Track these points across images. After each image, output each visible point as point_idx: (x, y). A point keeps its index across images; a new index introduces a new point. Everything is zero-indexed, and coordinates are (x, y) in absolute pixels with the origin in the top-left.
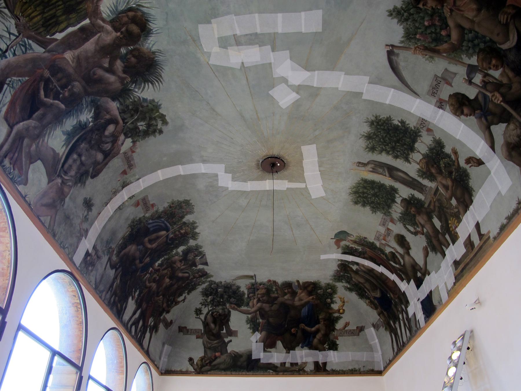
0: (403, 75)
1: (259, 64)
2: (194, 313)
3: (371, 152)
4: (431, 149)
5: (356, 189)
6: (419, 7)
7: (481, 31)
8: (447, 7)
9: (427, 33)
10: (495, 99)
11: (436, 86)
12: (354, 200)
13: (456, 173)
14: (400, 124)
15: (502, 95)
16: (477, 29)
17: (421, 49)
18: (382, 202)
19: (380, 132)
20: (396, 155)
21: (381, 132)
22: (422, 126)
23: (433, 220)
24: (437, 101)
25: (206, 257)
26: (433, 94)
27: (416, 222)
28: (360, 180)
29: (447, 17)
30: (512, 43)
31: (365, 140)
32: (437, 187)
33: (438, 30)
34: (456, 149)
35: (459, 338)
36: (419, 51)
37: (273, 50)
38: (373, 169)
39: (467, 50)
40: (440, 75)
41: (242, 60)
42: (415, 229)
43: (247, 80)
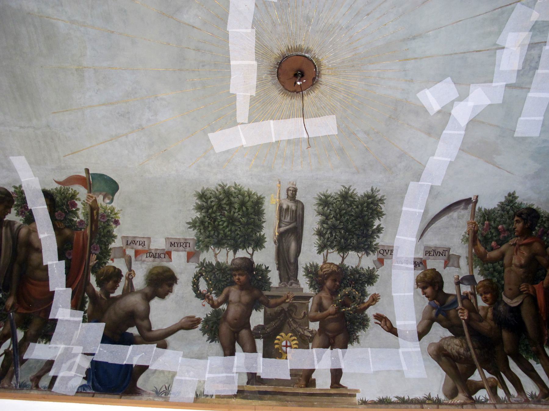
0: (442, 217)
1: (496, 69)
4: (356, 271)
5: (235, 193)
6: (515, 217)
7: (506, 275)
8: (517, 240)
9: (491, 230)
10: (460, 312)
11: (438, 252)
12: (208, 193)
13: (350, 310)
14: (375, 227)
15: (469, 316)
16: (506, 270)
17: (474, 228)
18: (222, 232)
19: (357, 207)
20: (324, 232)
21: (356, 209)
22: (382, 252)
23: (254, 311)
24: (421, 259)
26: (427, 252)
27: (224, 287)
28: (259, 195)
29: (508, 243)
30: (512, 304)
31: (341, 192)
32: (310, 297)
33: (495, 238)
34: (379, 299)
36: (472, 227)
37: (508, 86)
38: (288, 209)
39: (485, 269)
40: (451, 253)
41: (507, 48)
43: (477, 51)
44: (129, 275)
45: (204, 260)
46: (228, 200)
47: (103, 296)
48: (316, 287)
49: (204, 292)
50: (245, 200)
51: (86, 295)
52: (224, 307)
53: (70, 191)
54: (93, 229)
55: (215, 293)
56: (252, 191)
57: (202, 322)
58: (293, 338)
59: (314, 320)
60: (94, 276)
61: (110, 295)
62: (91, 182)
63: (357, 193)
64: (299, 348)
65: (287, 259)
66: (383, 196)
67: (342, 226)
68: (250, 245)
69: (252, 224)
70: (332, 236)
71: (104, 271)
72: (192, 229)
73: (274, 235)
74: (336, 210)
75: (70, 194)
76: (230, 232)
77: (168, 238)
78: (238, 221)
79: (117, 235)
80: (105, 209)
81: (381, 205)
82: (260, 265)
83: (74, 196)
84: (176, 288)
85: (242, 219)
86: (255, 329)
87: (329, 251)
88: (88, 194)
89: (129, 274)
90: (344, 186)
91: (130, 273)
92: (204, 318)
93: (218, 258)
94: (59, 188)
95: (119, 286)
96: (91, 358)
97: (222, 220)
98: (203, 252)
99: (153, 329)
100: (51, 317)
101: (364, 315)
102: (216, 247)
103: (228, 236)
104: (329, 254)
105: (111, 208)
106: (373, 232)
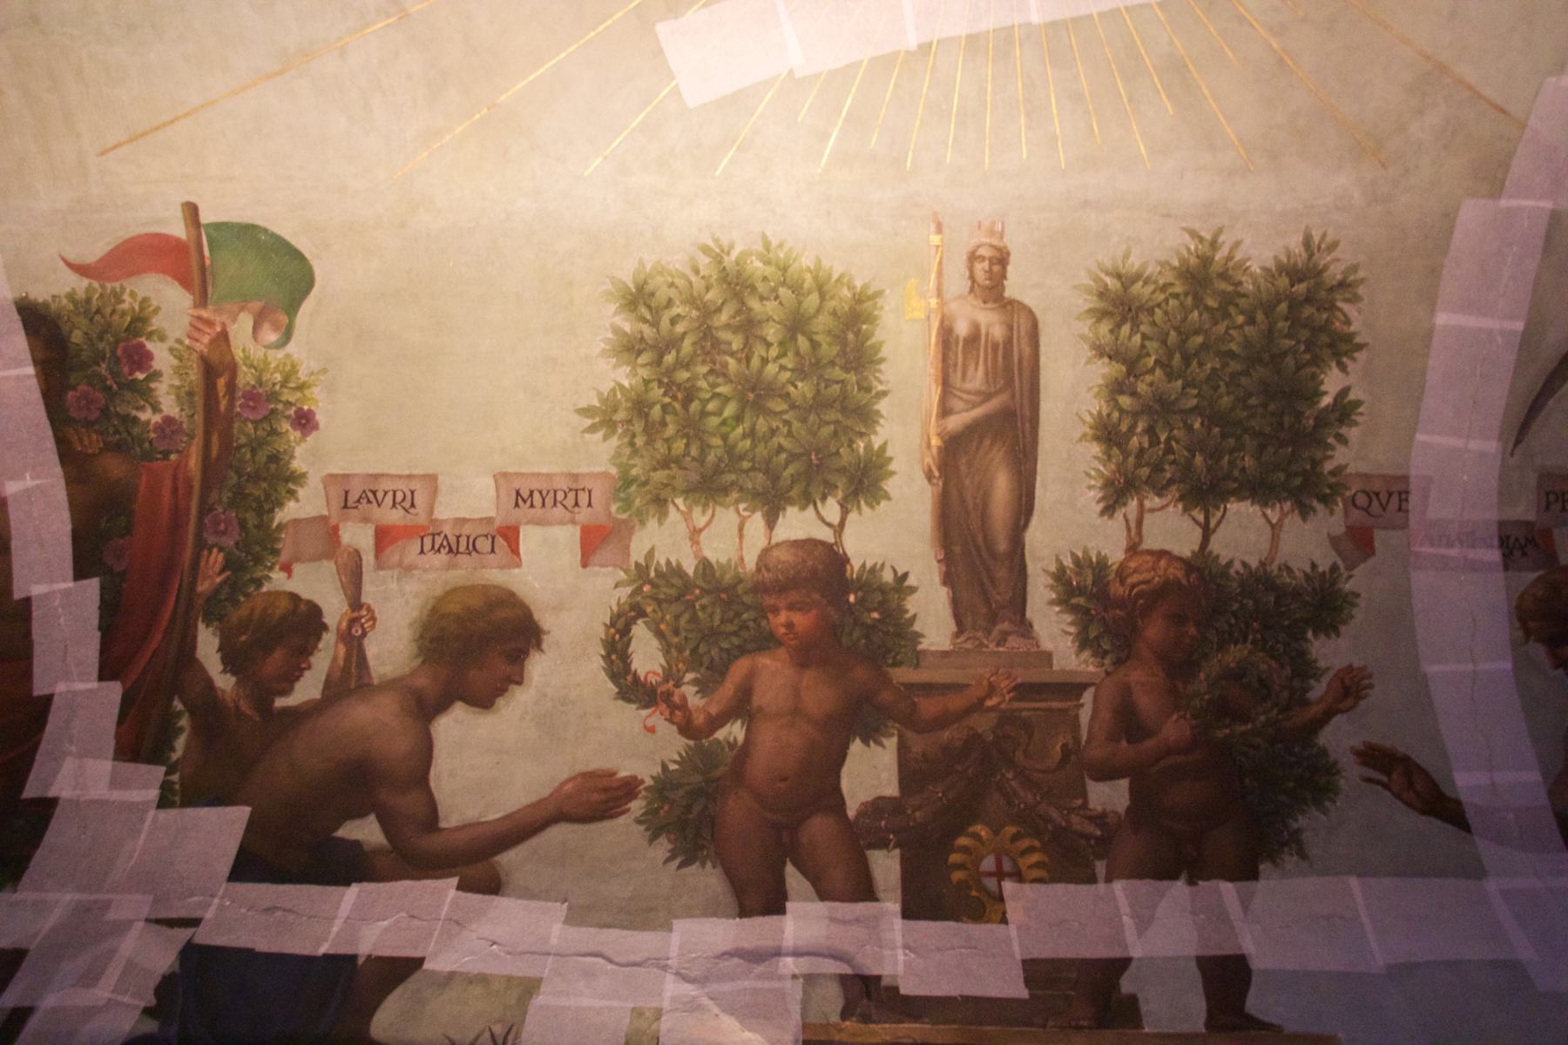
3: (1101, 305)
4: (1261, 581)
5: (765, 279)
12: (658, 283)
18: (717, 441)
19: (1251, 320)
20: (1124, 428)
21: (1247, 329)
22: (1362, 500)
23: (856, 746)
24: (1529, 524)
26: (1552, 497)
27: (731, 656)
28: (858, 284)
32: (1083, 687)
34: (1371, 686)
38: (973, 339)
44: (350, 628)
45: (650, 554)
46: (738, 312)
47: (245, 706)
48: (1106, 647)
49: (653, 679)
50: (805, 305)
51: (178, 705)
52: (735, 731)
53: (124, 301)
54: (214, 452)
55: (695, 682)
56: (831, 268)
57: (643, 793)
58: (1025, 843)
59: (1106, 773)
60: (214, 634)
61: (273, 702)
62: (208, 262)
63: (1249, 259)
64: (1054, 880)
65: (980, 539)
66: (1354, 268)
67: (1194, 402)
68: (829, 488)
69: (837, 405)
70: (1154, 441)
71: (252, 610)
72: (600, 435)
73: (924, 446)
74: (1167, 334)
75: (123, 314)
76: (748, 443)
77: (505, 475)
78: (780, 396)
79: (304, 470)
80: (260, 370)
81: (1345, 307)
82: (873, 570)
83: (139, 323)
84: (538, 667)
85: (796, 387)
86: (861, 814)
87: (1147, 504)
88: (196, 313)
89: (353, 621)
90: (1194, 234)
91: (356, 614)
92: (652, 777)
93: (702, 546)
94: (81, 294)
95: (309, 668)
96: (183, 935)
97: (716, 396)
98: (643, 523)
99: (443, 825)
100: (31, 791)
101: (1315, 750)
102: (696, 503)
103: (741, 458)
104: (1148, 519)
105: (285, 364)
106: (1322, 420)
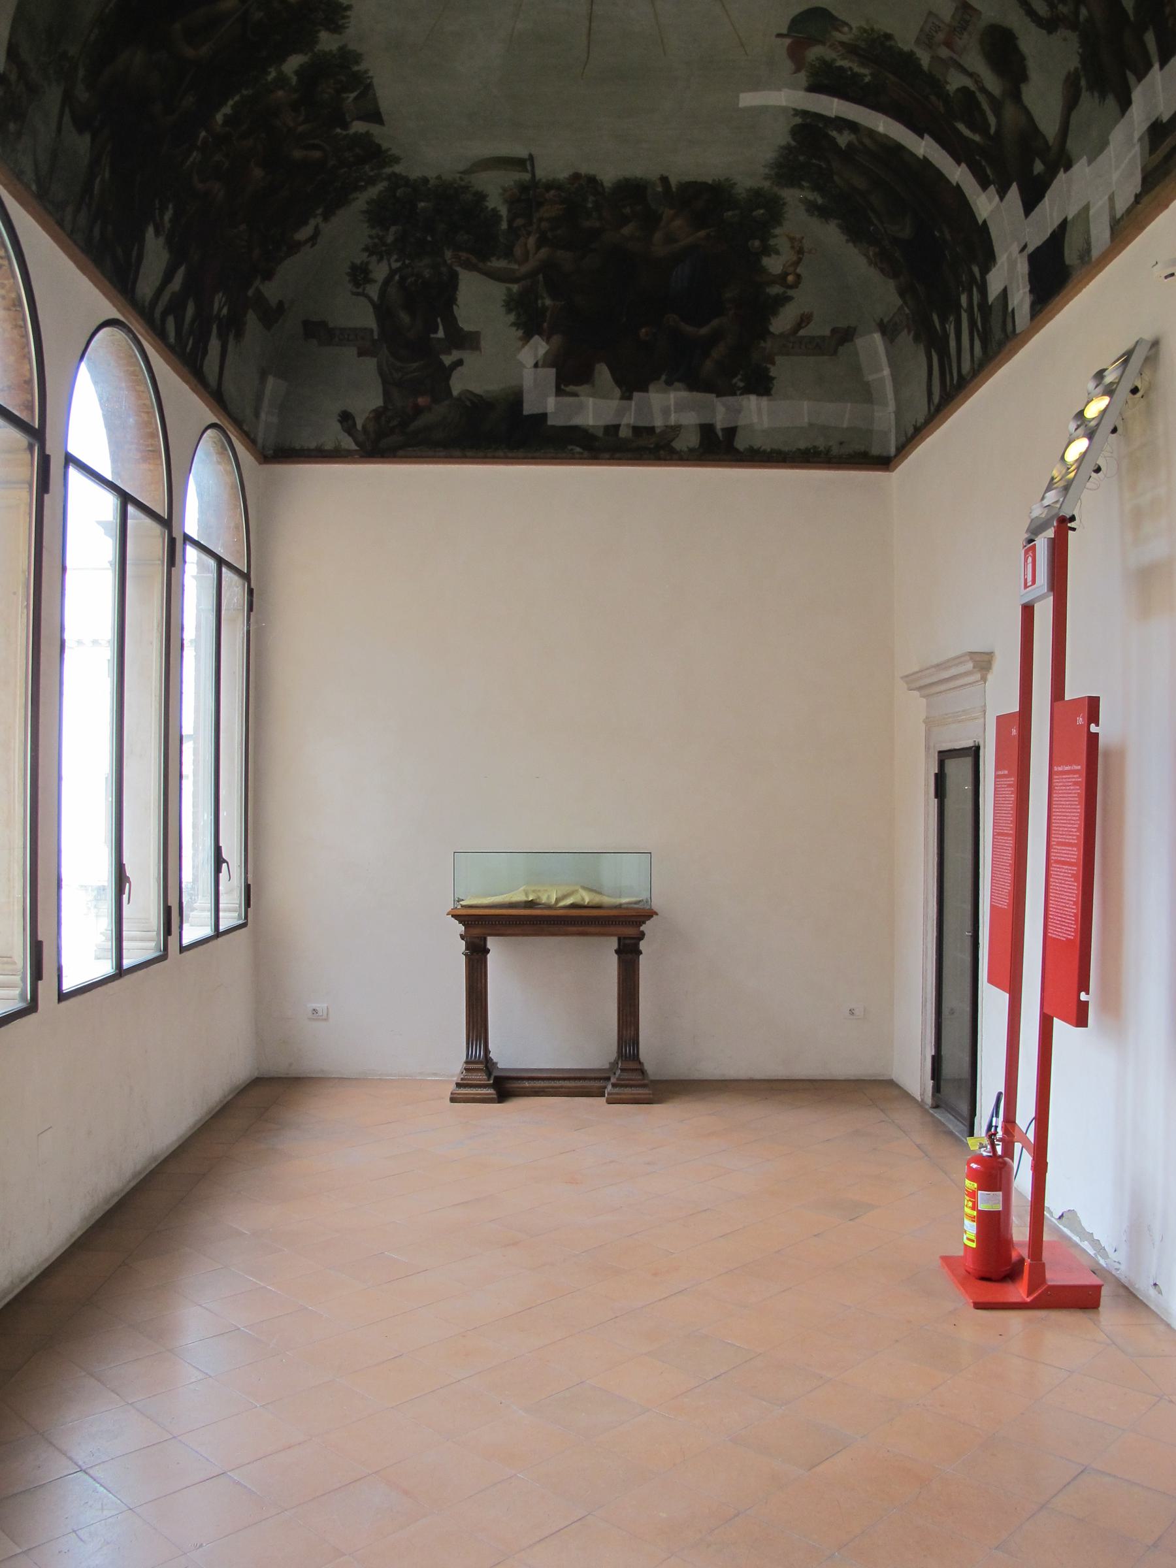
2: (348, 278)
25: (375, 95)
35: (1113, 364)
42: (1052, 6)
